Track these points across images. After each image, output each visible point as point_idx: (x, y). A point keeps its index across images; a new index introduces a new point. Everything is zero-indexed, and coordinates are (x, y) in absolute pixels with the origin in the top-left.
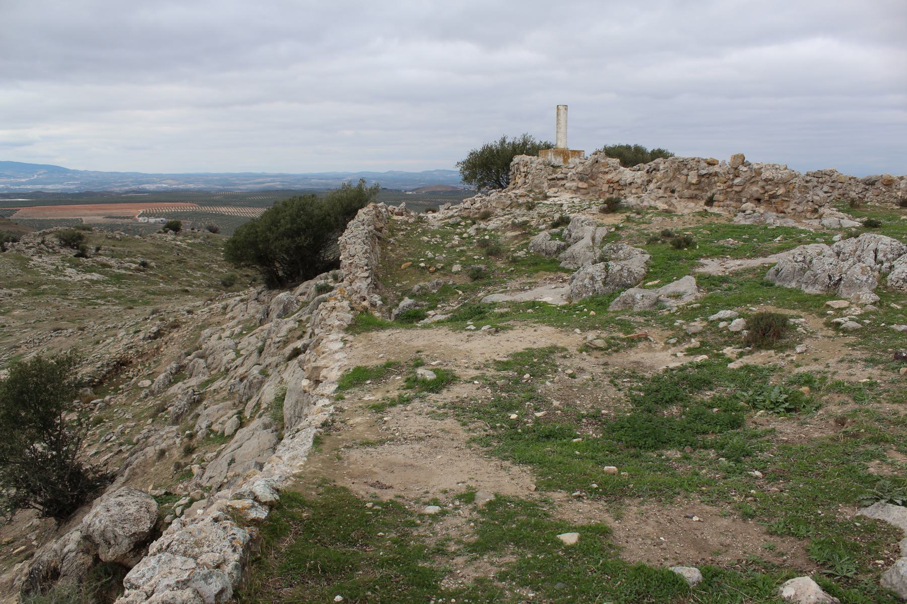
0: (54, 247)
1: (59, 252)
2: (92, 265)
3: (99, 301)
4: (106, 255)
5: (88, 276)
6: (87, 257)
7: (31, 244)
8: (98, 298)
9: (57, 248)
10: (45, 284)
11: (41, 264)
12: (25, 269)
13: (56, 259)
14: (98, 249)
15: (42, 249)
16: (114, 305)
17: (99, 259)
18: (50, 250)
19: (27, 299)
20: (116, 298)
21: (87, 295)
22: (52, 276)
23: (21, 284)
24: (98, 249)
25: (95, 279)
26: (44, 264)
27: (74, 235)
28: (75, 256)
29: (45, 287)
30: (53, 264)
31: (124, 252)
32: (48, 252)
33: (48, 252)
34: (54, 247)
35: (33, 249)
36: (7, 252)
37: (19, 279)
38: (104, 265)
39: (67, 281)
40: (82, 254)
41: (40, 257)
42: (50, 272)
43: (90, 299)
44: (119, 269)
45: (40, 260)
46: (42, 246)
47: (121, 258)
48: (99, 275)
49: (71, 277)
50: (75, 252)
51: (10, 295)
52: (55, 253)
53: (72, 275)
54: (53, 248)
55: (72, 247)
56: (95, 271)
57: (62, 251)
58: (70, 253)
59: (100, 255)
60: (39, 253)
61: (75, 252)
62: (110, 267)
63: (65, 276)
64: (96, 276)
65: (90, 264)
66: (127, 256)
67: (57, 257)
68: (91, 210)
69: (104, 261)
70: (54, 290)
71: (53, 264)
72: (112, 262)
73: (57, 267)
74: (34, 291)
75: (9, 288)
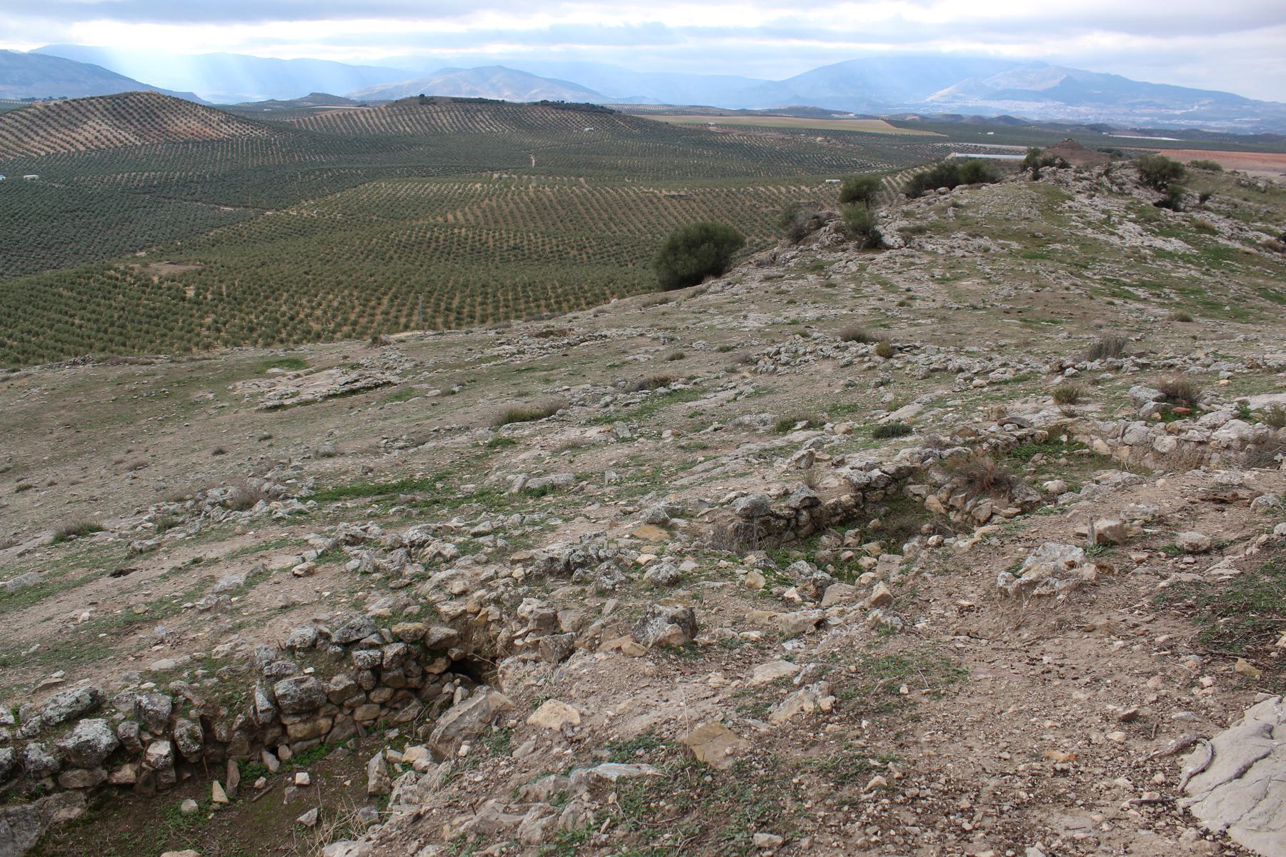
0: (1124, 184)
1: (1130, 194)
2: (1179, 225)
3: (1141, 293)
4: (1218, 212)
5: (1158, 242)
6: (1176, 209)
7: (1086, 174)
8: (1143, 284)
9: (1129, 186)
10: (1064, 241)
11: (1084, 209)
12: (1049, 211)
13: (1115, 205)
14: (1204, 198)
15: (1101, 184)
16: (1162, 305)
17: (1196, 216)
18: (1115, 188)
19: (1005, 264)
20: (1181, 291)
21: (1124, 276)
22: (1089, 230)
23: (1018, 236)
24: (1204, 198)
25: (1169, 247)
26: (1088, 209)
27: (1165, 167)
28: (1155, 205)
29: (1058, 246)
30: (1103, 212)
31: (1257, 211)
32: (1110, 191)
33: (1110, 191)
34: (1124, 184)
35: (1084, 182)
36: (1040, 181)
37: (1023, 225)
38: (1202, 228)
39: (1107, 243)
40: (1171, 203)
41: (1091, 197)
42: (1090, 223)
43: (1125, 284)
44: (1229, 239)
45: (1087, 202)
46: (1104, 179)
47: (1247, 222)
48: (1181, 243)
49: (1122, 238)
50: (1159, 197)
51: (987, 250)
52: (1122, 193)
53: (1131, 234)
54: (1121, 185)
55: (1158, 189)
56: (1177, 236)
57: (1135, 192)
58: (1148, 197)
59: (1207, 209)
60: (1093, 190)
61: (1159, 197)
62: (1214, 232)
63: (1112, 234)
64: (1174, 245)
65: (1179, 220)
66: (1261, 219)
67: (1120, 201)
68: (1264, 161)
69: (1207, 221)
70: (1070, 254)
71: (1103, 212)
72: (1224, 225)
73: (1109, 217)
74: (1033, 250)
75: (994, 236)
